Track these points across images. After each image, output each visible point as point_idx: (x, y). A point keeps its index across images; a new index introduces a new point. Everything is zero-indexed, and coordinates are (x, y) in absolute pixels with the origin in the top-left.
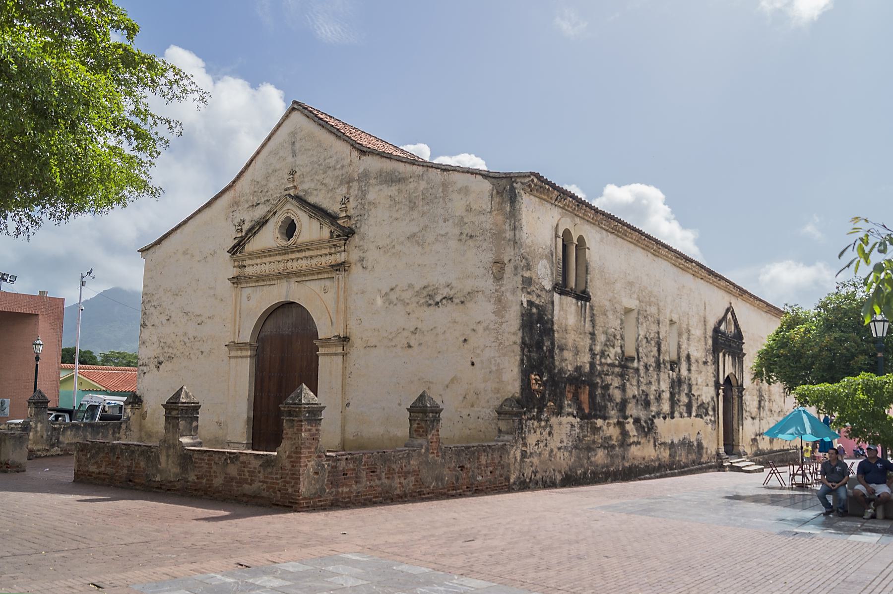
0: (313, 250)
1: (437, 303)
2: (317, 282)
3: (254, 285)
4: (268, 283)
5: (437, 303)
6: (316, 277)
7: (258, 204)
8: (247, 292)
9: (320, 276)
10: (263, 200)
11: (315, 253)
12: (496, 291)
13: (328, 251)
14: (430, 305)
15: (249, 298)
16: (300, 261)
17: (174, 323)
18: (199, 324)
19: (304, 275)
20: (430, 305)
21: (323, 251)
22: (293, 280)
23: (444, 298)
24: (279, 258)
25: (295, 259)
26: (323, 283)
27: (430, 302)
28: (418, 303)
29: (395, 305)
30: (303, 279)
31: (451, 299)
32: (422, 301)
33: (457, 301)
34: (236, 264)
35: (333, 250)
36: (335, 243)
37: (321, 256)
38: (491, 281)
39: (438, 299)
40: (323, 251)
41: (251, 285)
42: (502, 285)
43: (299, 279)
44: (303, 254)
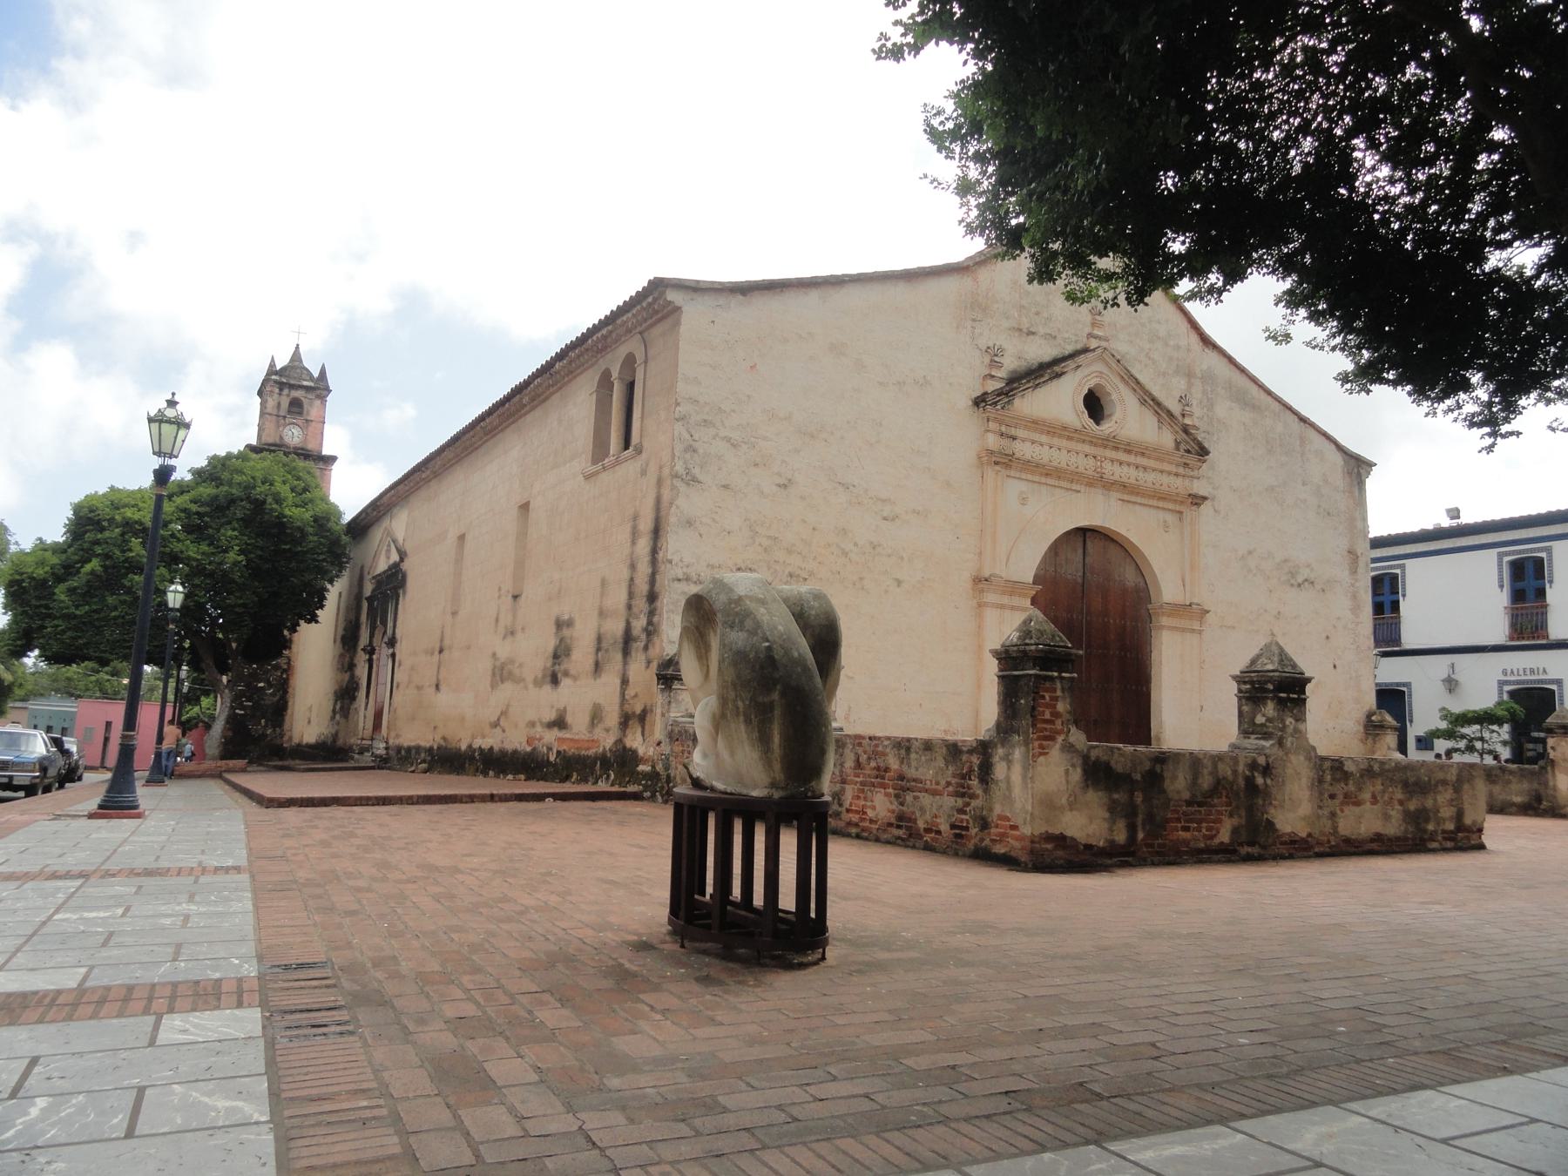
0: (1149, 458)
1: (1299, 585)
2: (1153, 511)
3: (1037, 478)
4: (1068, 485)
5: (1299, 585)
6: (1155, 503)
7: (1030, 333)
8: (1014, 487)
9: (1161, 504)
10: (1042, 330)
11: (1152, 463)
12: (1353, 585)
13: (1173, 469)
14: (1292, 585)
15: (1024, 501)
16: (1125, 469)
17: (803, 498)
18: (885, 519)
19: (1138, 494)
20: (1292, 585)
21: (1166, 467)
22: (1115, 495)
23: (1306, 580)
24: (1087, 448)
25: (1117, 460)
26: (1161, 515)
27: (1293, 581)
28: (1279, 579)
29: (1255, 575)
30: (1133, 498)
31: (1312, 583)
32: (1284, 578)
33: (1318, 587)
34: (992, 425)
35: (1181, 470)
36: (1188, 462)
37: (1162, 472)
38: (1347, 573)
39: (1300, 581)
40: (1166, 467)
41: (1030, 477)
42: (1356, 580)
43: (1126, 497)
44: (1131, 458)
